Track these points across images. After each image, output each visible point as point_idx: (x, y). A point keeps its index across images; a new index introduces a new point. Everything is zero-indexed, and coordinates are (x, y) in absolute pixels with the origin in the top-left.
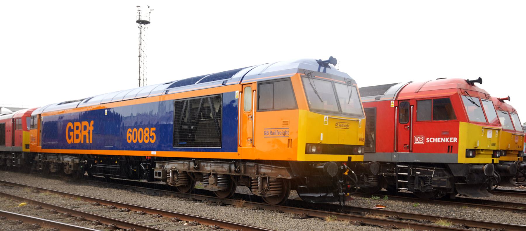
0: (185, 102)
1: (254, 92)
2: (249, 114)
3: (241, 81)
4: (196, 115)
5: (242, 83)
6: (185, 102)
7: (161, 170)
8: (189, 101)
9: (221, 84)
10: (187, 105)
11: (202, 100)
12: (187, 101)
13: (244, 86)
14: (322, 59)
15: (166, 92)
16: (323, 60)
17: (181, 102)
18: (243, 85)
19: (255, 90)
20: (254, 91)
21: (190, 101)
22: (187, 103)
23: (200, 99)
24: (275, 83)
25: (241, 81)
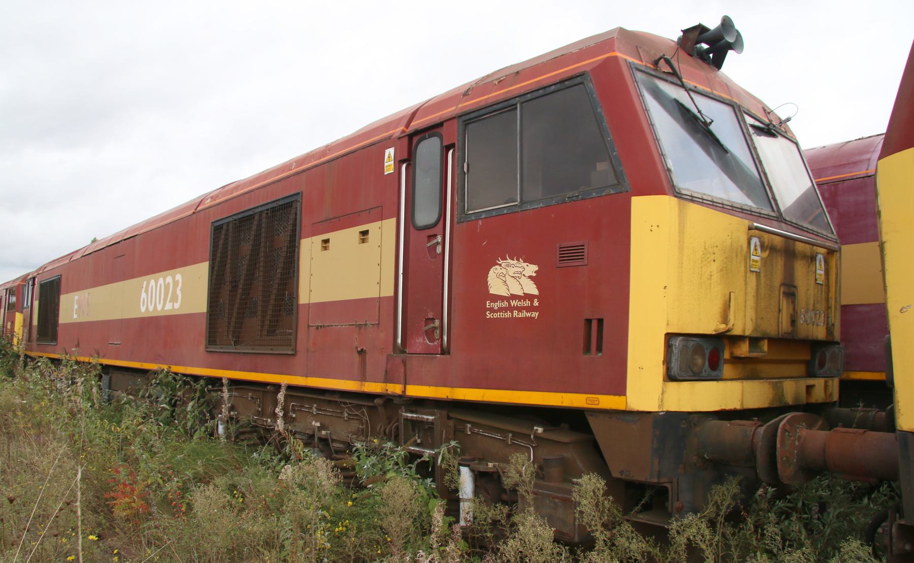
0: (257, 217)
1: (451, 152)
6: (257, 217)
8: (264, 215)
10: (259, 225)
13: (415, 140)
18: (411, 136)
20: (448, 148)
22: (260, 220)
24: (524, 104)
25: (407, 125)
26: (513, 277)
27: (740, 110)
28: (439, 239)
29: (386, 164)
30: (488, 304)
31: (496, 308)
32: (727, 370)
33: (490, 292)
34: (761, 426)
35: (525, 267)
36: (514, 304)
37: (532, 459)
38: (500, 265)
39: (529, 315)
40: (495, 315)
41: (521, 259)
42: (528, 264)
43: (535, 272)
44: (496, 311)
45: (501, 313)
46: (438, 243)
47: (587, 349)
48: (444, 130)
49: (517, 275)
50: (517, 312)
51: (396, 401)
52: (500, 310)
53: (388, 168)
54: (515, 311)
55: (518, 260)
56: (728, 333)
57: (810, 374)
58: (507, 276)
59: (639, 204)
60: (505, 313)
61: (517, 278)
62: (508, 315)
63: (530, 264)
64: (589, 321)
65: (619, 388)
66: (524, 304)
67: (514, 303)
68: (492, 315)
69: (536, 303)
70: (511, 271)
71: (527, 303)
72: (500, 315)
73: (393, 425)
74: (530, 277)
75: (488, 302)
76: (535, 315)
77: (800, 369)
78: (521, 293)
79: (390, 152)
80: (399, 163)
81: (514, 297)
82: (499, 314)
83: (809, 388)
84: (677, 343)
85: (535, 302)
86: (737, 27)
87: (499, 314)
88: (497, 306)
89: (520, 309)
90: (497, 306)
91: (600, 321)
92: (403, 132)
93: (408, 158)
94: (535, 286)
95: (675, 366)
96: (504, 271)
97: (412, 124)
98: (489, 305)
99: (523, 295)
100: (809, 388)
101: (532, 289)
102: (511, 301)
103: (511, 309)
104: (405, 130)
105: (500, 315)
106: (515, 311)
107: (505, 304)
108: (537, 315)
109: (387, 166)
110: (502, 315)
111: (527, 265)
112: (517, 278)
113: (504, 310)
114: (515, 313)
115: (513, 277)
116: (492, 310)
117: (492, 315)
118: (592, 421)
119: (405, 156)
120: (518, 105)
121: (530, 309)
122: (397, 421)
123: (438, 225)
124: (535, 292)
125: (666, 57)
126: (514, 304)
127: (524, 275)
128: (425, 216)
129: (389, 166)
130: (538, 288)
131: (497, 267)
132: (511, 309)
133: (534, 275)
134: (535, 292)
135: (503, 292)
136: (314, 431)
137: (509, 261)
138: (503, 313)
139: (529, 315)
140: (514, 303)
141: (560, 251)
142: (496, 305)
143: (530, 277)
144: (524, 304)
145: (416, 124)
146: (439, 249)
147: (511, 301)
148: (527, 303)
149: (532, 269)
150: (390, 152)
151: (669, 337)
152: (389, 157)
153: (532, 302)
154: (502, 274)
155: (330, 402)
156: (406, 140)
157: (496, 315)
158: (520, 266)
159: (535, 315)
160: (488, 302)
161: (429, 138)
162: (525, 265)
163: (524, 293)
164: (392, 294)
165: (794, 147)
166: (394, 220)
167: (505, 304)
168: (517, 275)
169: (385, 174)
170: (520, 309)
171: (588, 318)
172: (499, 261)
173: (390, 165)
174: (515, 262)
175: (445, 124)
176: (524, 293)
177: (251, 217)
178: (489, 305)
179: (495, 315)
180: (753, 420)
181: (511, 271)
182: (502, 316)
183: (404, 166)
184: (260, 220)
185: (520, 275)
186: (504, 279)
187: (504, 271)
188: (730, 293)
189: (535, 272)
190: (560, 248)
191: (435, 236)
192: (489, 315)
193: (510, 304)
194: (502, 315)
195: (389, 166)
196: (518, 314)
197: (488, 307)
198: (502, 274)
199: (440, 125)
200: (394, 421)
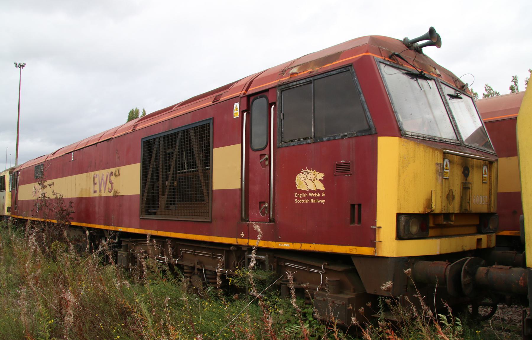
0: (157, 140)
1: (273, 107)
2: (262, 152)
3: (247, 90)
4: (171, 162)
5: (248, 93)
7: (126, 253)
8: (162, 139)
9: (212, 102)
11: (180, 134)
12: (159, 138)
13: (252, 99)
14: (408, 38)
15: (134, 127)
16: (411, 38)
17: (151, 141)
18: (249, 97)
19: (274, 103)
20: (271, 105)
21: (164, 137)
23: (176, 134)
24: (315, 81)
25: (247, 90)
26: (310, 180)
27: (438, 81)
28: (267, 156)
29: (234, 112)
30: (296, 195)
31: (301, 197)
32: (431, 232)
33: (297, 188)
34: (450, 264)
35: (317, 174)
36: (311, 195)
37: (322, 282)
38: (303, 173)
39: (319, 201)
40: (300, 201)
41: (315, 171)
42: (318, 173)
43: (323, 177)
44: (301, 199)
45: (304, 200)
46: (266, 159)
47: (352, 221)
48: (270, 94)
49: (313, 179)
50: (312, 199)
51: (244, 249)
52: (303, 198)
53: (235, 114)
54: (311, 199)
55: (313, 170)
56: (432, 213)
57: (480, 232)
58: (307, 179)
59: (381, 140)
60: (306, 200)
61: (313, 181)
62: (308, 201)
63: (320, 173)
64: (353, 206)
65: (372, 243)
66: (316, 195)
68: (299, 201)
69: (323, 195)
70: (309, 176)
72: (303, 201)
73: (241, 262)
74: (320, 180)
75: (296, 194)
76: (323, 201)
77: (473, 230)
78: (314, 189)
79: (237, 105)
80: (242, 113)
81: (311, 191)
82: (302, 200)
83: (479, 241)
84: (403, 218)
85: (323, 194)
86: (437, 32)
87: (302, 200)
88: (301, 196)
89: (314, 198)
90: (301, 196)
91: (360, 205)
92: (244, 94)
93: (247, 109)
94: (323, 185)
95: (402, 233)
96: (305, 176)
97: (249, 90)
98: (296, 196)
99: (316, 190)
100: (479, 241)
101: (321, 187)
102: (309, 193)
103: (310, 198)
104: (246, 92)
105: (303, 201)
106: (311, 199)
107: (306, 195)
108: (324, 202)
109: (235, 113)
110: (304, 201)
111: (318, 174)
112: (313, 181)
114: (312, 200)
115: (310, 180)
116: (298, 199)
117: (299, 201)
118: (355, 261)
119: (245, 108)
120: (313, 81)
121: (320, 198)
122: (244, 259)
123: (266, 149)
124: (323, 189)
125: (396, 53)
126: (311, 195)
127: (316, 179)
128: (258, 142)
129: (236, 114)
130: (324, 186)
131: (301, 174)
132: (310, 198)
133: (322, 179)
134: (323, 189)
135: (305, 188)
136: (195, 265)
137: (308, 171)
138: (305, 200)
139: (319, 201)
141: (337, 166)
142: (301, 196)
143: (320, 180)
144: (316, 195)
145: (251, 90)
146: (267, 163)
147: (309, 193)
149: (321, 176)
150: (237, 105)
151: (399, 215)
152: (236, 108)
153: (321, 194)
154: (304, 178)
155: (203, 248)
156: (245, 99)
157: (301, 201)
158: (314, 174)
159: (323, 201)
160: (296, 194)
161: (260, 98)
162: (317, 173)
163: (316, 189)
164: (239, 187)
165: (470, 99)
166: (240, 144)
167: (306, 195)
168: (313, 179)
169: (234, 118)
170: (314, 198)
171: (352, 203)
172: (302, 171)
173: (237, 113)
174: (311, 171)
175: (270, 90)
176: (316, 189)
177: (154, 139)
178: (296, 196)
179: (300, 201)
180: (445, 261)
181: (309, 176)
182: (304, 202)
183: (245, 114)
184: (159, 142)
185: (314, 179)
186: (305, 181)
187: (305, 176)
188: (432, 191)
189: (323, 177)
190: (336, 164)
191: (264, 155)
192: (296, 201)
193: (308, 195)
194: (304, 201)
195: (236, 114)
196: (313, 201)
197: (296, 196)
198: (304, 178)
199: (267, 90)
200: (241, 259)
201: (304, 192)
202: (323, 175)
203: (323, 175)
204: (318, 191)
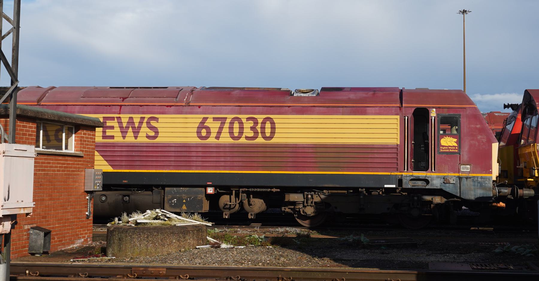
39: (454, 151)
44: (444, 149)
52: (445, 149)
55: (451, 137)
62: (448, 150)
67: (449, 148)
69: (457, 148)
71: (454, 148)
78: (452, 145)
101: (456, 145)
107: (447, 148)
113: (447, 149)
114: (450, 150)
116: (442, 149)
124: (457, 145)
134: (457, 145)
137: (448, 137)
139: (454, 151)
140: (449, 148)
142: (444, 148)
143: (454, 142)
148: (454, 148)
149: (455, 140)
153: (455, 148)
157: (444, 150)
162: (453, 139)
167: (447, 148)
174: (450, 138)
181: (449, 140)
193: (448, 148)
201: (446, 146)
202: (456, 140)
203: (456, 140)
204: (454, 146)
